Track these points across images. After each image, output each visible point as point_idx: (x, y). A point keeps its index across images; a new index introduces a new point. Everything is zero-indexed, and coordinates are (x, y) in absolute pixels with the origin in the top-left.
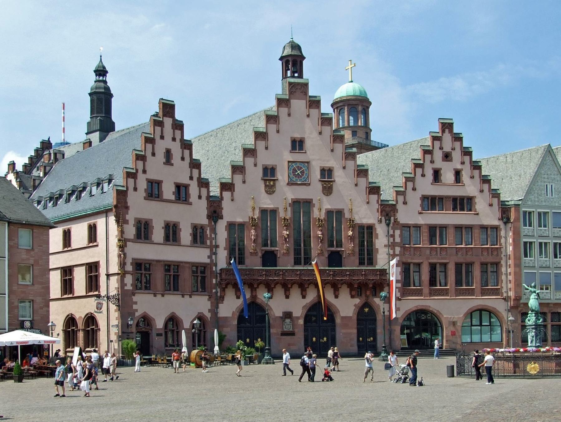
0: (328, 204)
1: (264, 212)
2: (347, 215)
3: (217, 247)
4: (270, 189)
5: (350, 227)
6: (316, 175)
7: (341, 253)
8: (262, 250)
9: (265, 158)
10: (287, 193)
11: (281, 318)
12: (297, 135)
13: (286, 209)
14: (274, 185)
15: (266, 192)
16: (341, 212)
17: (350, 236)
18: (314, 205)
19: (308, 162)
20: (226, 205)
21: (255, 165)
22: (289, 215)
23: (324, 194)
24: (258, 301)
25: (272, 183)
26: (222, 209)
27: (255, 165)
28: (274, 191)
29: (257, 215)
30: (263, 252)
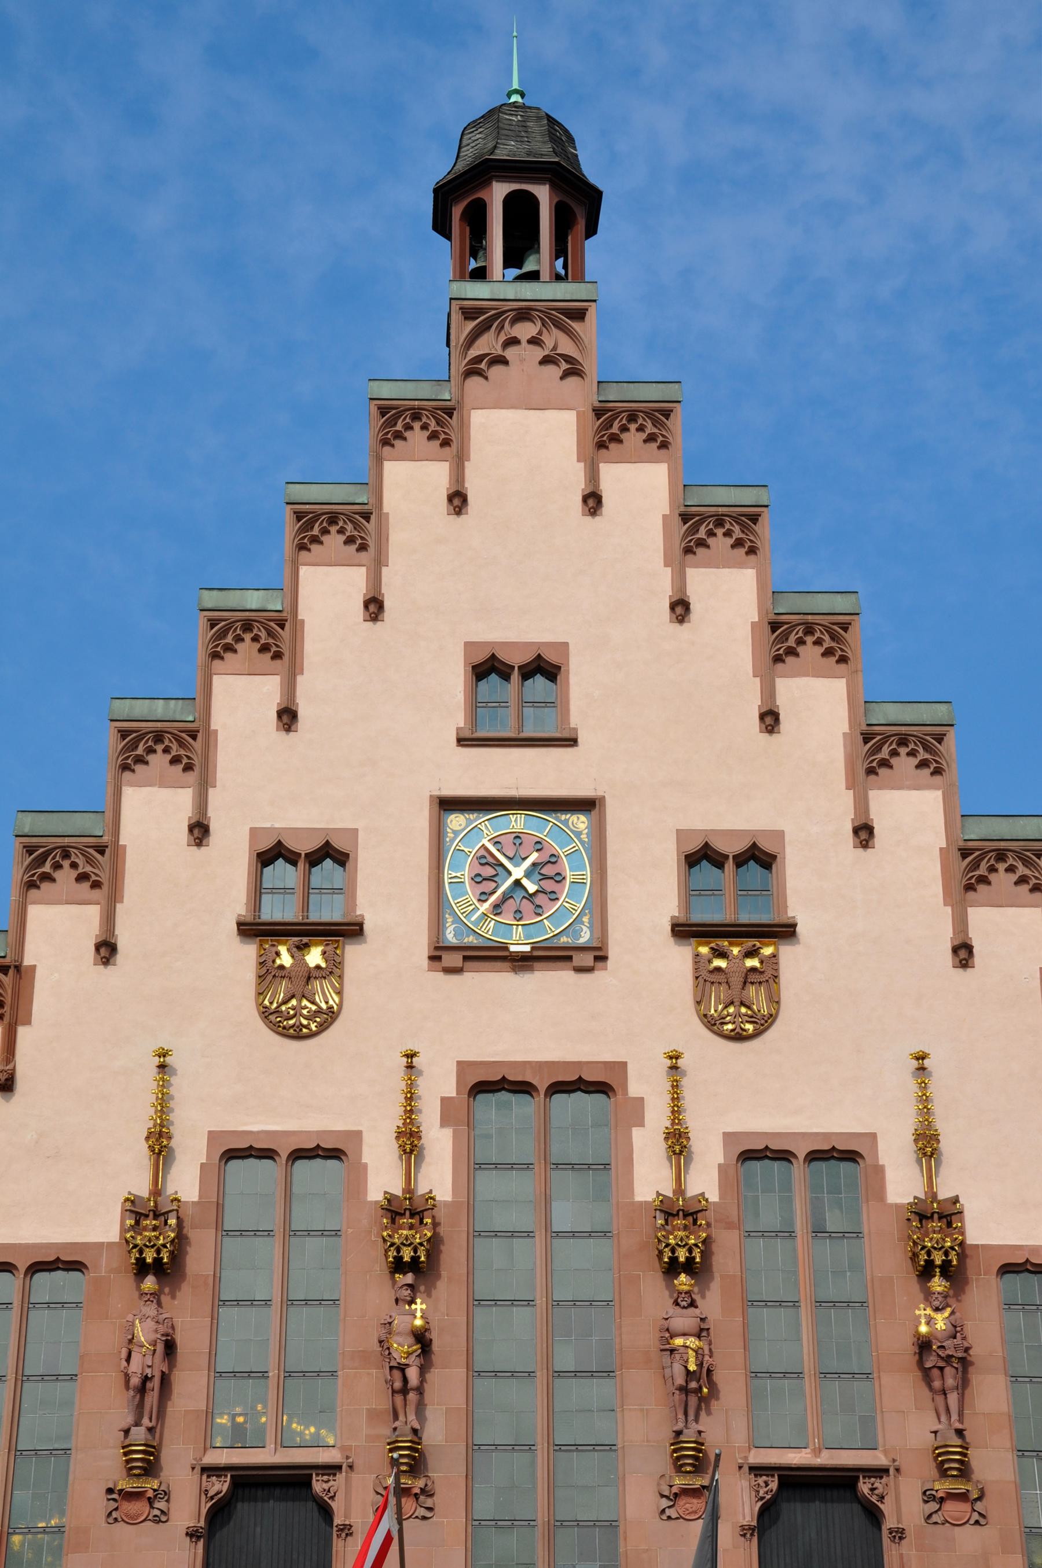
0: (747, 1095)
2: (903, 1185)
5: (926, 1272)
6: (647, 896)
7: (864, 1487)
8: (210, 1471)
12: (517, 631)
15: (275, 1020)
16: (851, 1156)
17: (924, 1345)
18: (636, 1111)
19: (586, 805)
21: (199, 831)
23: (712, 1024)
25: (314, 957)
27: (199, 831)
28: (329, 1017)
29: (185, 1183)
30: (221, 1486)
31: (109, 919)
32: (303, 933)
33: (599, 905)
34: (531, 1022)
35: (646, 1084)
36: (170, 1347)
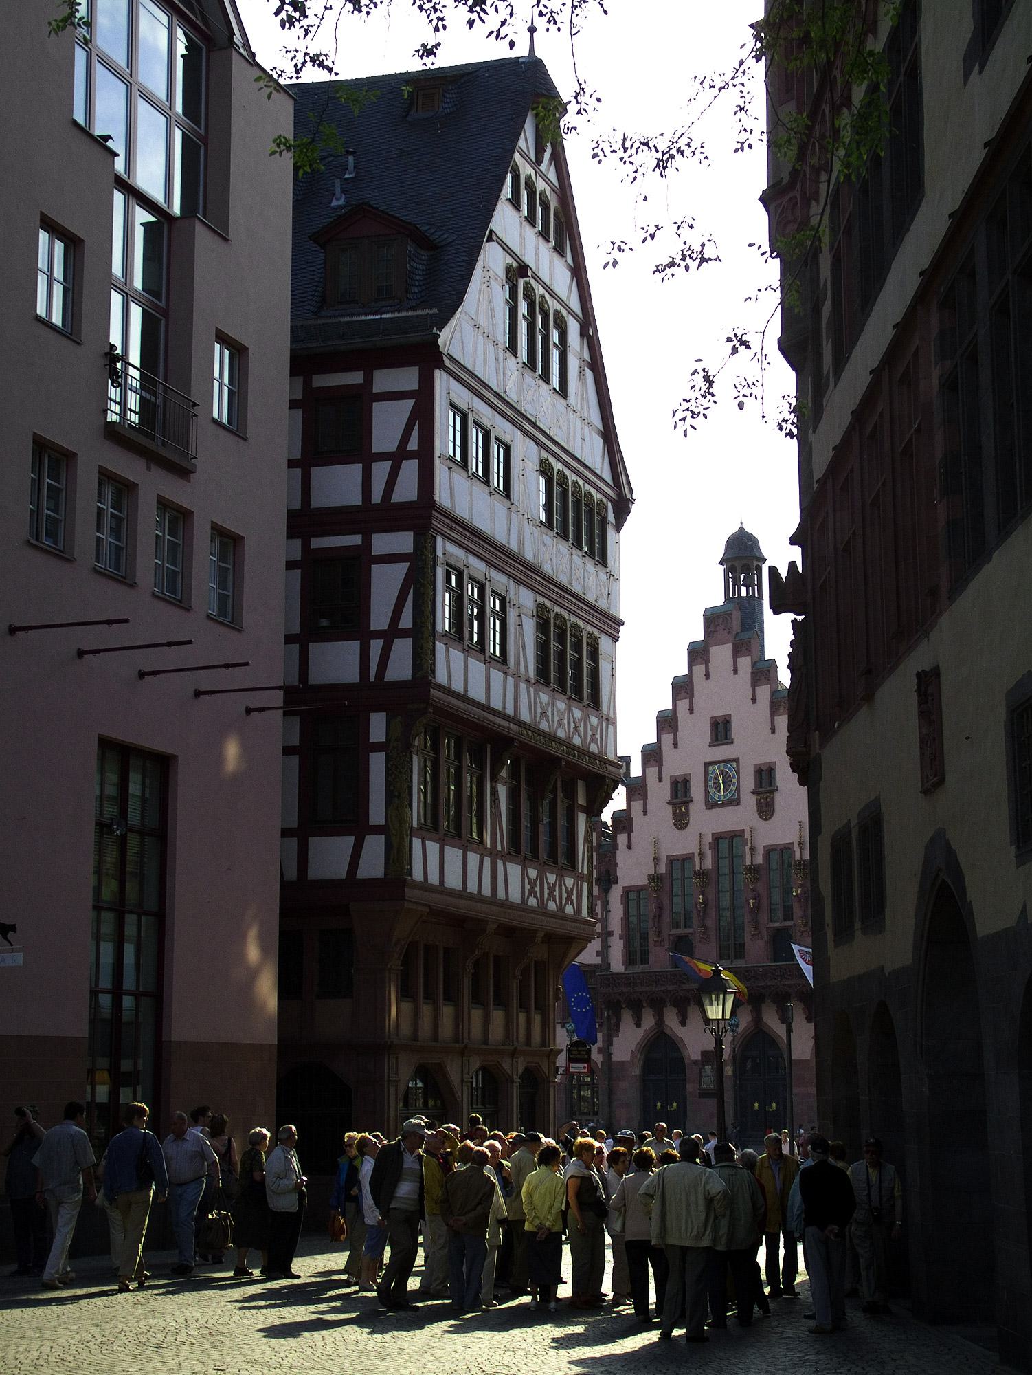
1: (672, 860)
3: (610, 934)
4: (681, 820)
9: (675, 765)
10: (706, 822)
11: (696, 1062)
13: (701, 854)
14: (687, 810)
19: (736, 760)
20: (622, 855)
21: (660, 779)
22: (708, 864)
24: (667, 1031)
26: (616, 865)
27: (660, 779)
28: (686, 825)
29: (662, 869)
31: (645, 804)
32: (682, 803)
33: (738, 788)
34: (727, 820)
35: (747, 836)
36: (660, 908)
